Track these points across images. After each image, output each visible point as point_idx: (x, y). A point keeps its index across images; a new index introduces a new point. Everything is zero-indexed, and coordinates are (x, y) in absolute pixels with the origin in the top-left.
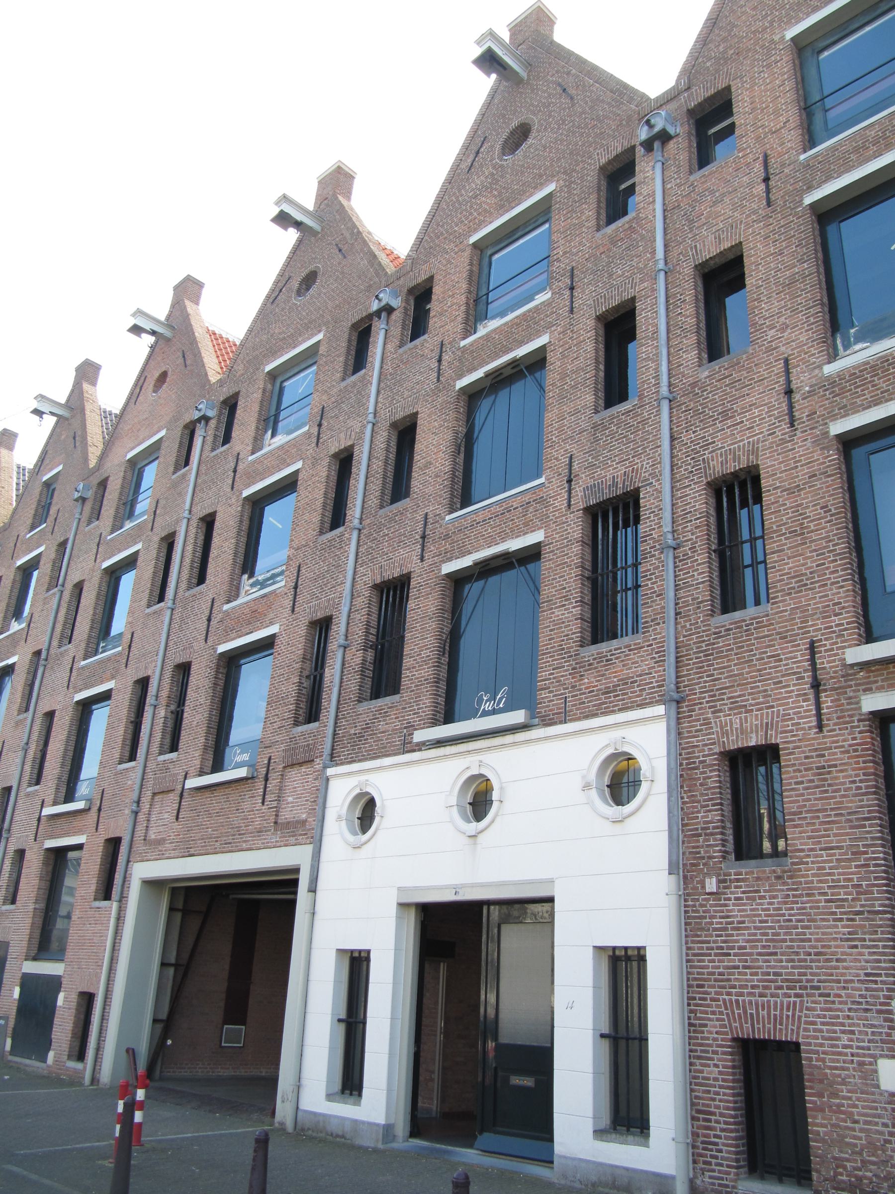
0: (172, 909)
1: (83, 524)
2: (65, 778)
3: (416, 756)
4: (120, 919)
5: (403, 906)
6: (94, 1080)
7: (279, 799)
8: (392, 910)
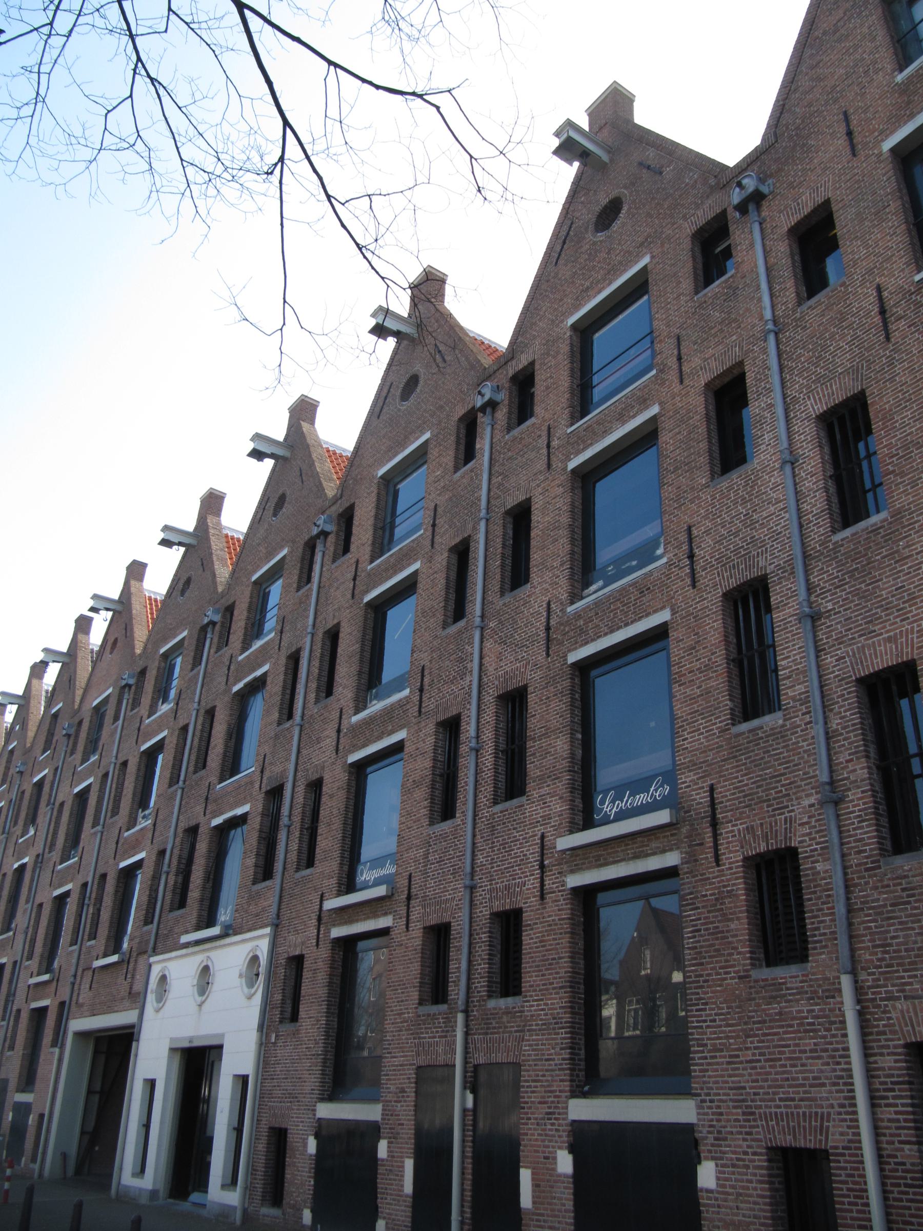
0: (96, 1052)
1: (68, 755)
2: (46, 954)
3: (184, 951)
4: (60, 1060)
5: (173, 1050)
6: (41, 1175)
7: (133, 977)
8: (165, 1053)
